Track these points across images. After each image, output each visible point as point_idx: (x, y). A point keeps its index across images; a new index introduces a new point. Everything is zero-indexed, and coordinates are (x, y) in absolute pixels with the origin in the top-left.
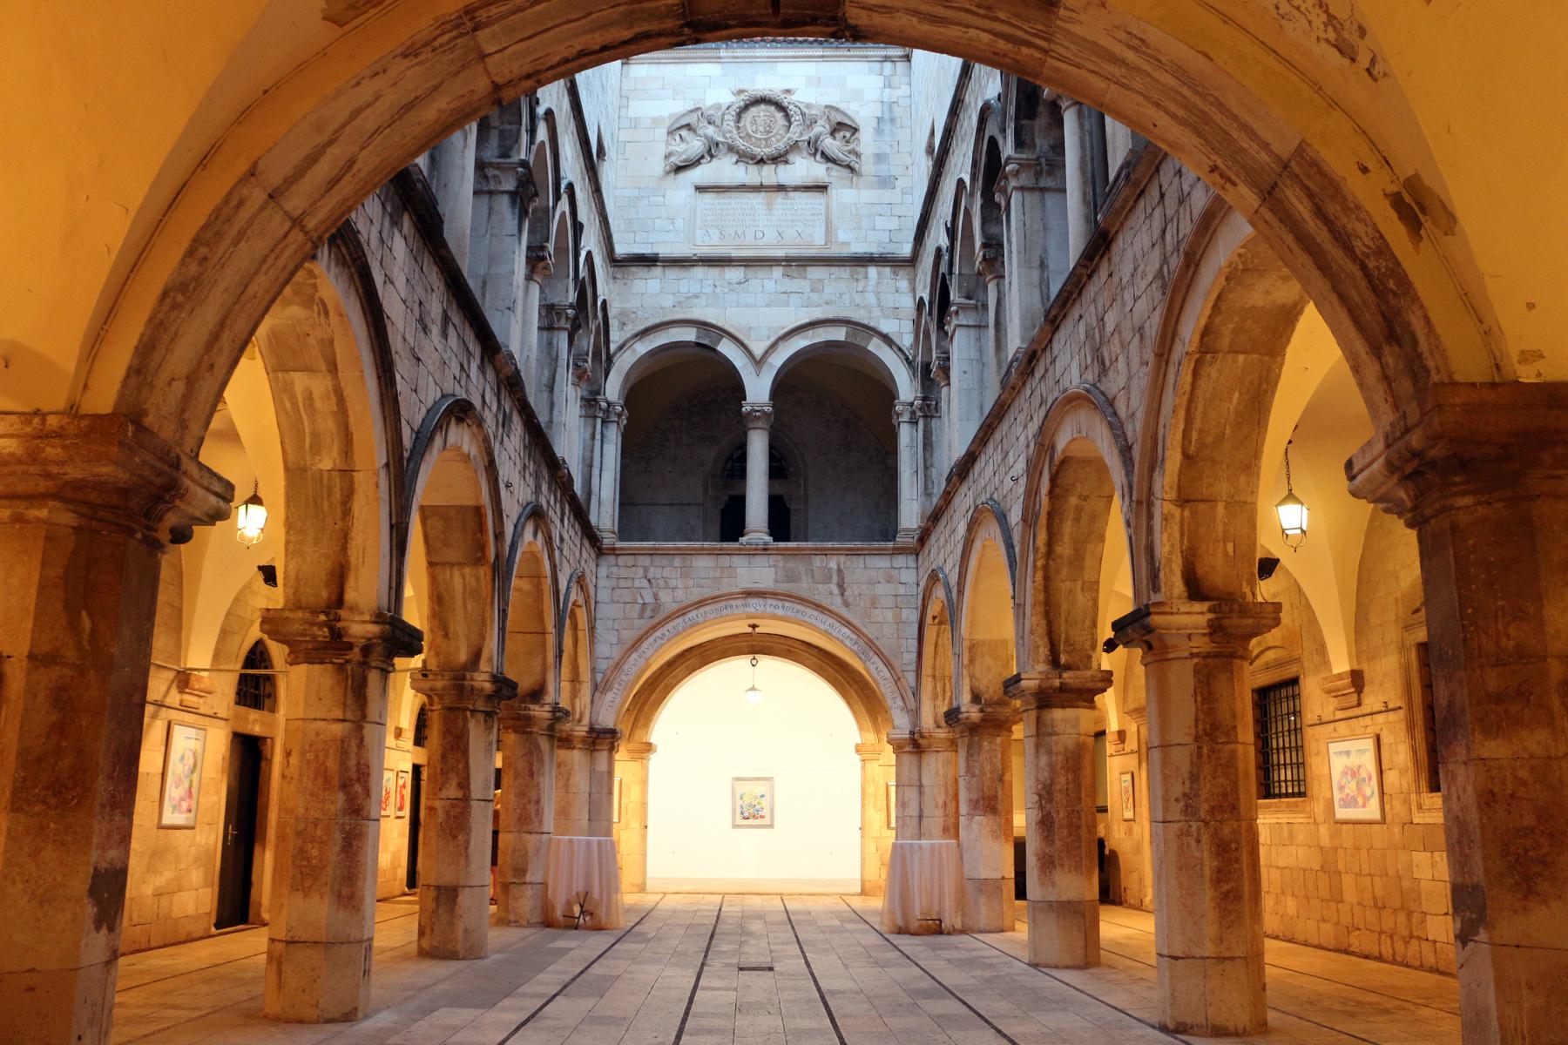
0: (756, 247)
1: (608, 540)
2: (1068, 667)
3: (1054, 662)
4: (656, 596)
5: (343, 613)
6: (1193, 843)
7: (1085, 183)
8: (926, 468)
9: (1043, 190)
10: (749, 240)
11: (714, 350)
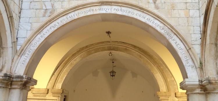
4: (53, 6)
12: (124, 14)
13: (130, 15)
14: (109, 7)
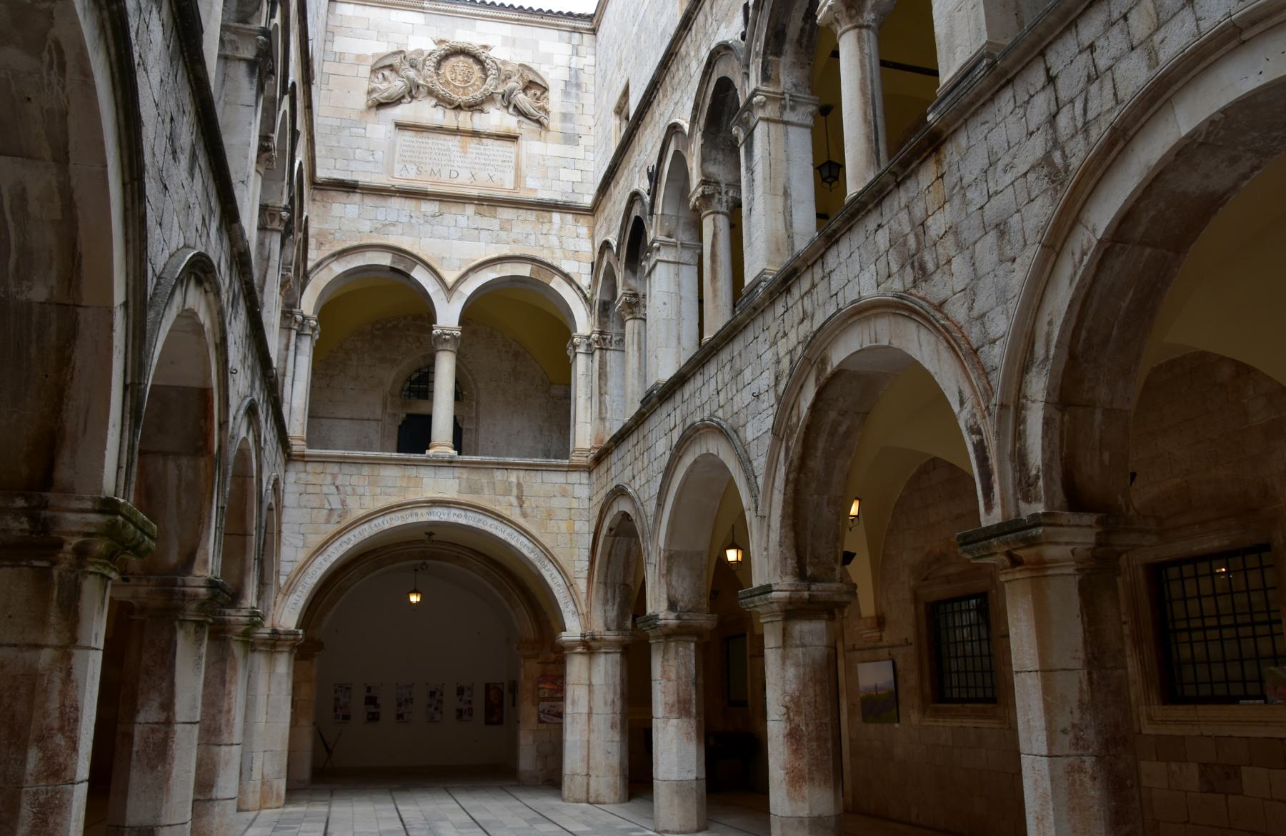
0: (451, 185)
1: (298, 447)
2: (814, 580)
3: (800, 573)
4: (343, 502)
5: (51, 497)
6: (1088, 783)
7: (865, 103)
8: (601, 394)
9: (786, 123)
10: (444, 177)
11: (408, 276)
12: (471, 523)
13: (480, 526)
14: (445, 510)
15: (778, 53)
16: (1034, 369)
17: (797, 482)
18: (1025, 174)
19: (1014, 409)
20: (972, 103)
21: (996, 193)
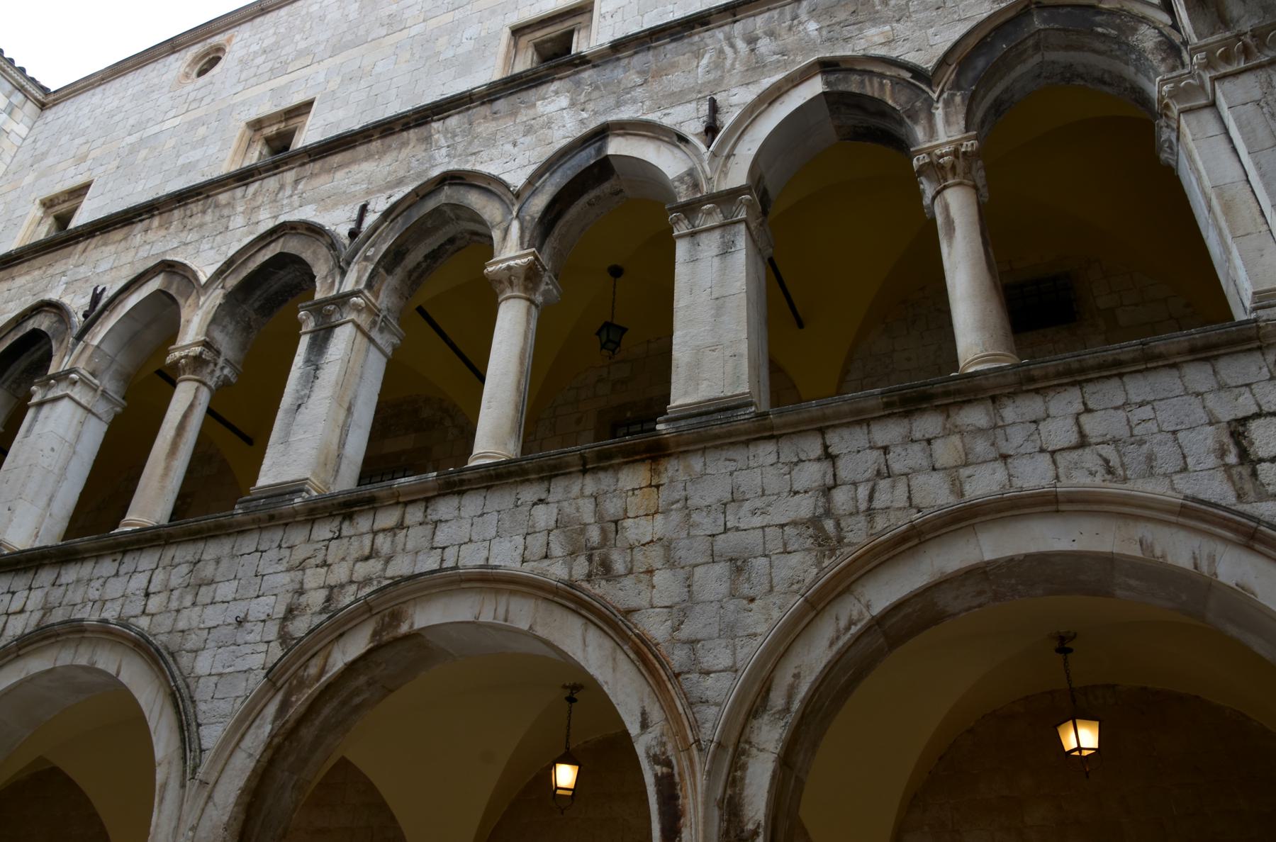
9: (371, 340)
15: (389, 271)
16: (766, 717)
17: (278, 748)
18: (782, 526)
19: (735, 752)
20: (717, 437)
21: (737, 529)
